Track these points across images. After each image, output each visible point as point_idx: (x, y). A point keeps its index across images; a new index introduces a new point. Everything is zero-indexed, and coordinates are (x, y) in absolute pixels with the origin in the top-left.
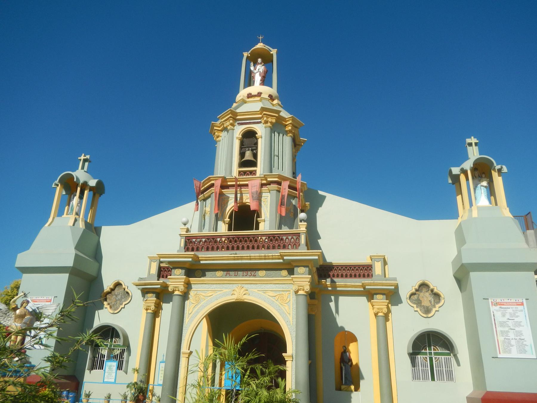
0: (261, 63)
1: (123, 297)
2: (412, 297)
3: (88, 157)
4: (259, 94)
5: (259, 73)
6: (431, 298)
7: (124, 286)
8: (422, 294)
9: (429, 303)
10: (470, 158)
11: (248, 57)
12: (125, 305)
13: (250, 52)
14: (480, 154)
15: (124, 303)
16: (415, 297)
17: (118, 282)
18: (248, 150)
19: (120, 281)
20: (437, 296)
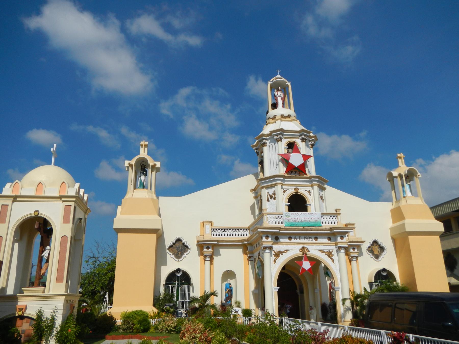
0: (280, 91)
1: (182, 249)
2: (369, 249)
3: (147, 143)
4: (289, 116)
5: (280, 97)
6: (379, 249)
7: (183, 242)
8: (374, 247)
9: (378, 252)
10: (400, 166)
11: (271, 84)
12: (186, 255)
13: (271, 80)
14: (407, 164)
15: (185, 254)
16: (370, 249)
17: (179, 238)
20: (382, 249)
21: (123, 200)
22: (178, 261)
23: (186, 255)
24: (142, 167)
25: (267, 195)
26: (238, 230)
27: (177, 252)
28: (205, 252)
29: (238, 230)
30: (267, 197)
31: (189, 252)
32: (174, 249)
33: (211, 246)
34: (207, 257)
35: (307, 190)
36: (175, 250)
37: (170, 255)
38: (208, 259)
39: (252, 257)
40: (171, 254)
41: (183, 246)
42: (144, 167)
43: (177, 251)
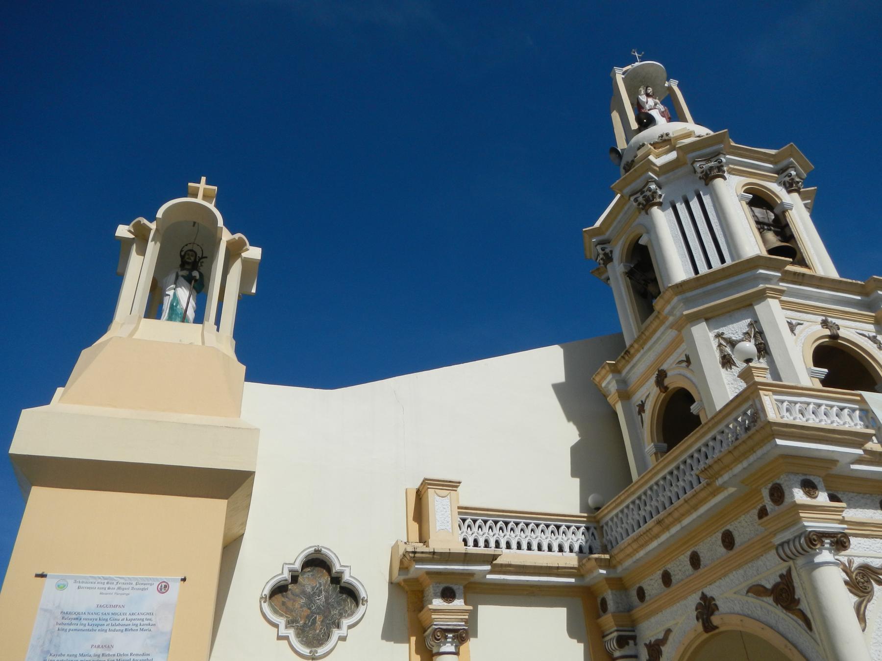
5: (657, 110)
7: (337, 567)
12: (350, 627)
15: (346, 622)
17: (318, 551)
18: (770, 230)
19: (323, 549)
21: (85, 353)
22: (313, 659)
23: (350, 627)
24: (187, 257)
25: (720, 345)
26: (558, 527)
27: (308, 617)
28: (436, 611)
29: (556, 526)
30: (721, 351)
31: (363, 615)
32: (294, 601)
33: (462, 587)
34: (446, 637)
35: (866, 333)
36: (297, 606)
37: (276, 626)
38: (449, 647)
39: (631, 642)
40: (281, 621)
41: (335, 589)
42: (193, 259)
43: (306, 612)
